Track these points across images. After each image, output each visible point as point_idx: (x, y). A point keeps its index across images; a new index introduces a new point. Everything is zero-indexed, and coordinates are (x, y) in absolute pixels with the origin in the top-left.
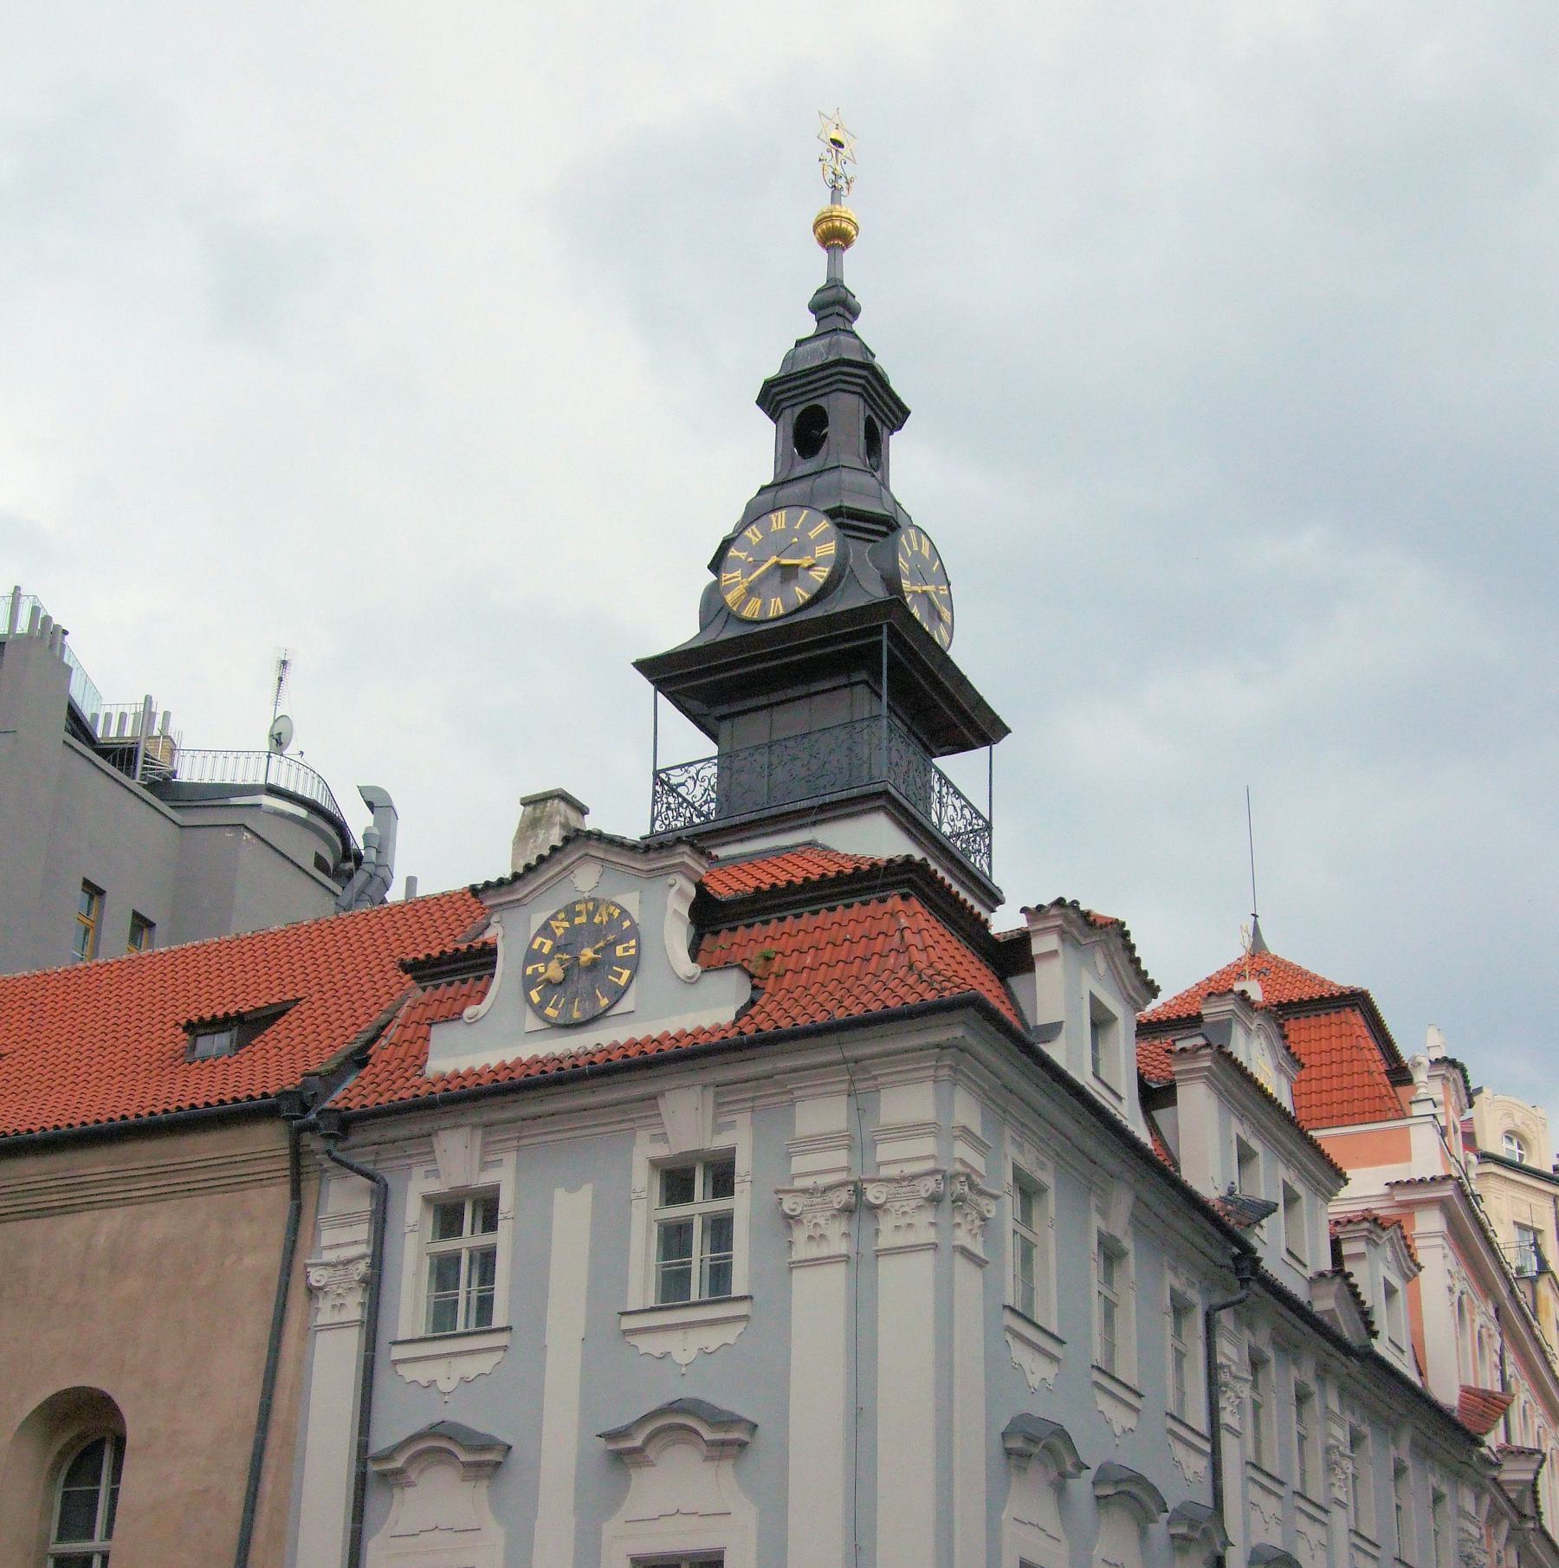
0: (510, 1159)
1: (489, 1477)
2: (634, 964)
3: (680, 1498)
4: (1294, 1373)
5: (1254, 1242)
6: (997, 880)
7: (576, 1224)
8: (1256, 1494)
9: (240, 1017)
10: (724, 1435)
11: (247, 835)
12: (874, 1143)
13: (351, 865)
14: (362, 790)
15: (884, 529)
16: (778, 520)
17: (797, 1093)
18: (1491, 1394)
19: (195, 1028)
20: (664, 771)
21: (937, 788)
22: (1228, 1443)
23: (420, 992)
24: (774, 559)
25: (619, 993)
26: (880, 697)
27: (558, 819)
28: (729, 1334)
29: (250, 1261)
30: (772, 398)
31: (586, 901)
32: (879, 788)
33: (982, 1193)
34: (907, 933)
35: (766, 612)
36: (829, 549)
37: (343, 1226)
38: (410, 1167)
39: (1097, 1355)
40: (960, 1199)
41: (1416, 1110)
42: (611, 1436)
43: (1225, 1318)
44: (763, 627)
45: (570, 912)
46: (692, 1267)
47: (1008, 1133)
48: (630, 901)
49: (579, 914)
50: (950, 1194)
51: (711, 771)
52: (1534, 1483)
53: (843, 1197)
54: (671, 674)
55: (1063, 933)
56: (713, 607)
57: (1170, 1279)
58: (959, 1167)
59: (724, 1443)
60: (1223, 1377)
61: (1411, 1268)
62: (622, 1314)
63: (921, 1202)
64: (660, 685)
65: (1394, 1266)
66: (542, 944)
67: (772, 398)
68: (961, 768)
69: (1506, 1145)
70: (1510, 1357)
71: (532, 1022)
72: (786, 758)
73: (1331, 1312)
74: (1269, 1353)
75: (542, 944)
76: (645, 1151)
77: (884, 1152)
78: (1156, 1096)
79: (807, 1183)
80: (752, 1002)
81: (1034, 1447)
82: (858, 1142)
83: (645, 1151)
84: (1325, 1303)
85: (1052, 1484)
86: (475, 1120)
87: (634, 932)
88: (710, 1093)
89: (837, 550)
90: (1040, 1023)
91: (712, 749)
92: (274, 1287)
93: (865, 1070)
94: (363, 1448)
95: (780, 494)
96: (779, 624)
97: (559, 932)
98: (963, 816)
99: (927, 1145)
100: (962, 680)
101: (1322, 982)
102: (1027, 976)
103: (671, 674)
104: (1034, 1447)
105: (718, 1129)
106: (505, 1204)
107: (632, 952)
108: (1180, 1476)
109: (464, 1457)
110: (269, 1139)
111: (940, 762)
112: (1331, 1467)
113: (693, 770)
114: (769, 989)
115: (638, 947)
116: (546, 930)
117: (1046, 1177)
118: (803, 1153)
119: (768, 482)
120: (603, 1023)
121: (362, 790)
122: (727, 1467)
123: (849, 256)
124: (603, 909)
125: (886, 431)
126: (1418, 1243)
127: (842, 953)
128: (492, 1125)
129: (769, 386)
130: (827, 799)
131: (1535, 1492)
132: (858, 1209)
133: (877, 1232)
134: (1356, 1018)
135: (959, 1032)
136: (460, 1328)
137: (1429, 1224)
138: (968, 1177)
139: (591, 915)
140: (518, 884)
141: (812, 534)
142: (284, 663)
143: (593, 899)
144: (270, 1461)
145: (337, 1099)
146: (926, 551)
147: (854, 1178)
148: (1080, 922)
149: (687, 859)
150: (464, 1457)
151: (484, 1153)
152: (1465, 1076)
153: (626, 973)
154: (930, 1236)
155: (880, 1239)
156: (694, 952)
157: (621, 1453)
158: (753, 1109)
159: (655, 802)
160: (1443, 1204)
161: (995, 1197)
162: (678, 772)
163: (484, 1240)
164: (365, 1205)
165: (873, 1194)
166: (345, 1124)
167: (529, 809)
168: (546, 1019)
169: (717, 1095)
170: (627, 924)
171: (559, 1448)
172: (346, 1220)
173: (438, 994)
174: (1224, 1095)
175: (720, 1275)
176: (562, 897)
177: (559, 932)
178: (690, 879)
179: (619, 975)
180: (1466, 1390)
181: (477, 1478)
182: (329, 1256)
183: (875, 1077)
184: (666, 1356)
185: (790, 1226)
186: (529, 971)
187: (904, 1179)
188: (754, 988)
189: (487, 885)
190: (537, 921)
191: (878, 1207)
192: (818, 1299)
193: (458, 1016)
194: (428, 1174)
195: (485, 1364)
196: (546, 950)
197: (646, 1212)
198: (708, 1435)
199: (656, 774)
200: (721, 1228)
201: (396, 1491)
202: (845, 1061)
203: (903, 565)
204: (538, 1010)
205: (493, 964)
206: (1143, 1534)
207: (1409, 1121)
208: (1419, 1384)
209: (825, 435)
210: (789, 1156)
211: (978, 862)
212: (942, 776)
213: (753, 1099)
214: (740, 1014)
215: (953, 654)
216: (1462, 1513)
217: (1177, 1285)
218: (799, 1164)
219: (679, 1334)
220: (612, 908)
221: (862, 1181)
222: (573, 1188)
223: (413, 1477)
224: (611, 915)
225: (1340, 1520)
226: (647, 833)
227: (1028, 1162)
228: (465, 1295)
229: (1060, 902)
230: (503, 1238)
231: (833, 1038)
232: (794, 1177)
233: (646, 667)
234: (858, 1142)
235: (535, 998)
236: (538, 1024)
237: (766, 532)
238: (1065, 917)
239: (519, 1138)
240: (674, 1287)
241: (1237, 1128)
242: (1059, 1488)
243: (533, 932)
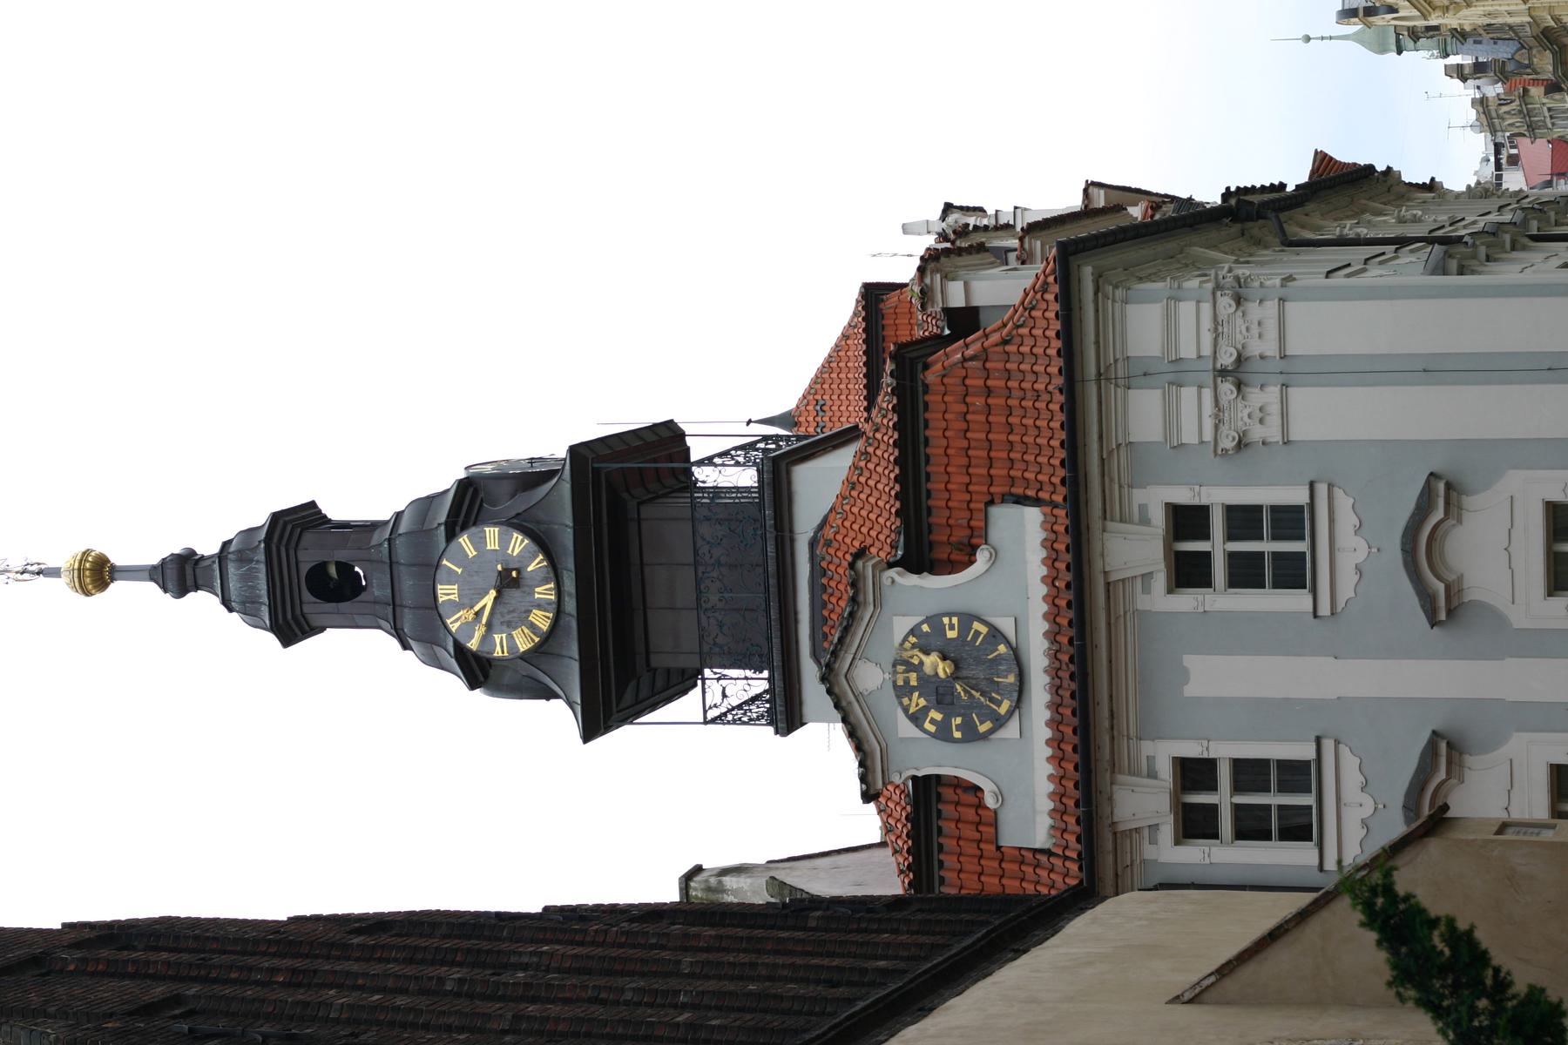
0: (1147, 748)
1: (1461, 754)
2: (967, 619)
3: (1496, 550)
15: (471, 491)
20: (705, 712)
25: (995, 634)
28: (1344, 503)
31: (895, 673)
35: (549, 602)
38: (1143, 861)
44: (571, 605)
45: (902, 691)
48: (901, 626)
49: (907, 681)
53: (1227, 388)
55: (946, 277)
62: (1315, 616)
63: (1239, 313)
66: (933, 721)
71: (1011, 730)
75: (933, 721)
77: (1187, 351)
79: (1208, 425)
80: (1022, 500)
82: (1175, 373)
83: (1160, 600)
87: (934, 620)
88: (1110, 525)
89: (495, 524)
93: (1108, 368)
95: (407, 602)
96: (569, 585)
97: (922, 702)
101: (845, 336)
102: (982, 317)
105: (1145, 521)
106: (1192, 750)
107: (955, 620)
109: (1442, 775)
115: (950, 615)
116: (917, 719)
118: (1179, 430)
120: (1023, 647)
122: (1469, 502)
123: (118, 559)
124: (906, 655)
132: (1238, 373)
133: (1262, 357)
135: (1087, 272)
141: (471, 552)
143: (894, 666)
147: (1208, 378)
150: (1442, 775)
151: (1137, 774)
153: (977, 626)
154: (1271, 307)
155: (1268, 353)
157: (1445, 607)
158: (1131, 486)
163: (1224, 775)
165: (1227, 359)
168: (1010, 713)
170: (925, 628)
171: (1440, 679)
177: (922, 702)
179: (977, 633)
181: (1461, 766)
184: (1359, 570)
185: (1246, 445)
186: (957, 735)
187: (1216, 329)
189: (863, 779)
190: (906, 728)
192: (1320, 415)
194: (1153, 841)
195: (1350, 763)
196: (938, 716)
198: (1439, 514)
199: (706, 722)
200: (1243, 520)
202: (1098, 380)
204: (1000, 722)
209: (339, 565)
218: (1189, 436)
219: (1339, 556)
220: (907, 645)
221: (1214, 369)
222: (1185, 675)
224: (914, 646)
226: (771, 729)
230: (1225, 751)
231: (1078, 386)
232: (1202, 442)
233: (588, 734)
234: (1175, 373)
236: (1014, 724)
240: (1292, 573)
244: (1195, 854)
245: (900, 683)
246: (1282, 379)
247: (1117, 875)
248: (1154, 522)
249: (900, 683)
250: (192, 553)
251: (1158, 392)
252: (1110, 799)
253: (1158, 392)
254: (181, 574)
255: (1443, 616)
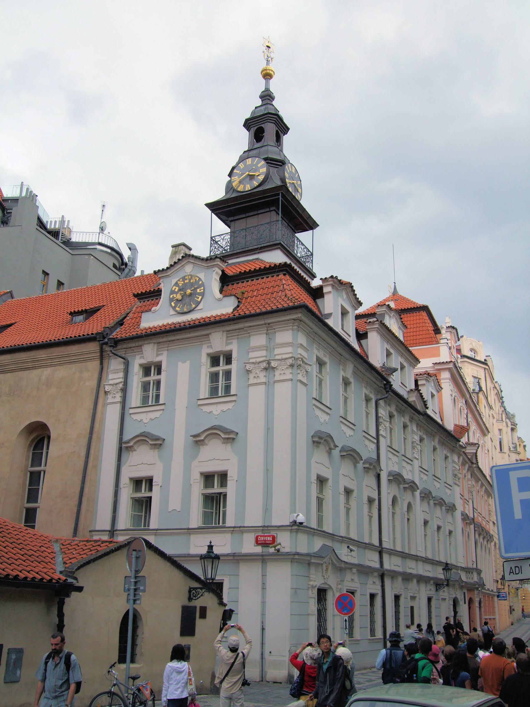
2: (203, 294)
4: (403, 419)
5: (390, 380)
6: (315, 270)
7: (184, 372)
8: (390, 455)
9: (86, 311)
10: (228, 436)
11: (92, 257)
12: (274, 349)
13: (124, 267)
14: (127, 244)
15: (281, 164)
16: (249, 161)
17: (251, 334)
18: (463, 427)
19: (73, 314)
21: (296, 242)
22: (381, 439)
23: (139, 303)
24: (247, 173)
25: (198, 303)
26: (279, 215)
27: (182, 252)
28: (230, 406)
29: (87, 384)
30: (248, 124)
32: (278, 242)
33: (306, 364)
34: (285, 285)
35: (245, 189)
36: (264, 170)
37: (115, 373)
38: (135, 355)
39: (342, 413)
40: (300, 365)
41: (442, 341)
42: (194, 436)
43: (382, 402)
45: (184, 279)
46: (219, 385)
47: (315, 346)
48: (202, 276)
49: (186, 279)
50: (297, 364)
51: (228, 237)
52: (476, 453)
53: (264, 365)
54: (216, 207)
55: (333, 286)
56: (229, 187)
57: (364, 391)
58: (299, 356)
59: (228, 438)
60: (381, 420)
61: (439, 388)
63: (288, 366)
64: (213, 211)
65: (434, 388)
66: (175, 289)
67: (248, 124)
68: (304, 236)
69: (470, 353)
70: (470, 416)
71: (172, 312)
72: (250, 233)
73: (414, 401)
74: (395, 413)
75: (175, 289)
76: (205, 351)
77: (277, 351)
78: (361, 336)
79: (254, 360)
80: (238, 306)
81: (321, 440)
82: (268, 348)
83: (205, 351)
84: (412, 398)
85: (327, 451)
86: (155, 341)
87: (203, 285)
88: (225, 333)
89: (267, 170)
90: (326, 313)
91: (228, 230)
92: (95, 391)
94: (121, 439)
97: (180, 285)
98: (304, 251)
99: (290, 349)
100: (304, 210)
101: (414, 303)
103: (216, 207)
104: (321, 440)
105: (227, 344)
106: (163, 367)
107: (202, 291)
108: (367, 450)
109: (151, 442)
110: (93, 347)
111: (297, 235)
112: (413, 448)
113: (222, 237)
114: (243, 302)
115: (204, 289)
116: (176, 284)
117: (326, 359)
118: (252, 352)
119: (246, 150)
121: (127, 244)
122: (229, 446)
125: (282, 135)
126: (442, 381)
127: (265, 291)
128: (160, 343)
129: (247, 121)
130: (262, 245)
131: (476, 456)
132: (269, 368)
133: (274, 375)
134: (424, 314)
135: (299, 315)
136: (150, 404)
137: (445, 376)
138: (302, 359)
139: (190, 280)
140: (168, 270)
141: (259, 165)
142: (104, 206)
144: (93, 444)
145: (114, 335)
146: (294, 171)
148: (338, 283)
149: (219, 263)
150: (151, 442)
152: (457, 332)
153: (200, 297)
154: (290, 376)
156: (221, 291)
157: (198, 441)
158: (238, 338)
159: (211, 246)
160: (449, 369)
161: (310, 365)
162: (218, 237)
163: (158, 377)
164: (122, 367)
165: (273, 364)
166: (116, 342)
167: (174, 248)
168: (176, 311)
169: (227, 334)
170: (200, 282)
171: (179, 440)
172: (116, 371)
173: (144, 304)
174: (382, 335)
175: (228, 388)
176: (181, 274)
177: (180, 285)
178: (220, 269)
180: (456, 425)
181: (155, 448)
182: (111, 382)
183: (274, 329)
184: (211, 412)
186: (171, 296)
187: (282, 359)
188: (239, 302)
189: (159, 271)
190: (174, 281)
191: (275, 368)
192: (256, 396)
193: (150, 310)
195: (157, 414)
196: (176, 290)
197: (205, 369)
199: (211, 238)
200: (228, 374)
201: (131, 452)
203: (287, 175)
204: (174, 308)
205: (161, 294)
206: (355, 466)
207: (440, 345)
208: (441, 423)
210: (248, 352)
211: (308, 265)
212: (298, 239)
213: (238, 335)
214: (234, 310)
215: (302, 202)
216: (454, 462)
217: (367, 392)
218: (251, 355)
223: (136, 448)
224: (196, 280)
225: (416, 463)
226: (209, 255)
227: (321, 355)
228: (152, 394)
229: (332, 277)
230: (163, 377)
232: (250, 359)
233: (209, 205)
234: (268, 348)
235: (173, 305)
236: (174, 313)
237: (245, 165)
238: (334, 281)
239: (168, 347)
240: (214, 392)
241: (386, 346)
242: (329, 452)
243: (172, 285)
244: (136, 371)
245: (186, 278)
246: (267, 383)
247: (130, 348)
248: (227, 347)
249: (186, 278)
250: (273, 99)
251: (265, 344)
252: (149, 343)
253: (265, 344)
254: (267, 97)
255: (195, 439)
